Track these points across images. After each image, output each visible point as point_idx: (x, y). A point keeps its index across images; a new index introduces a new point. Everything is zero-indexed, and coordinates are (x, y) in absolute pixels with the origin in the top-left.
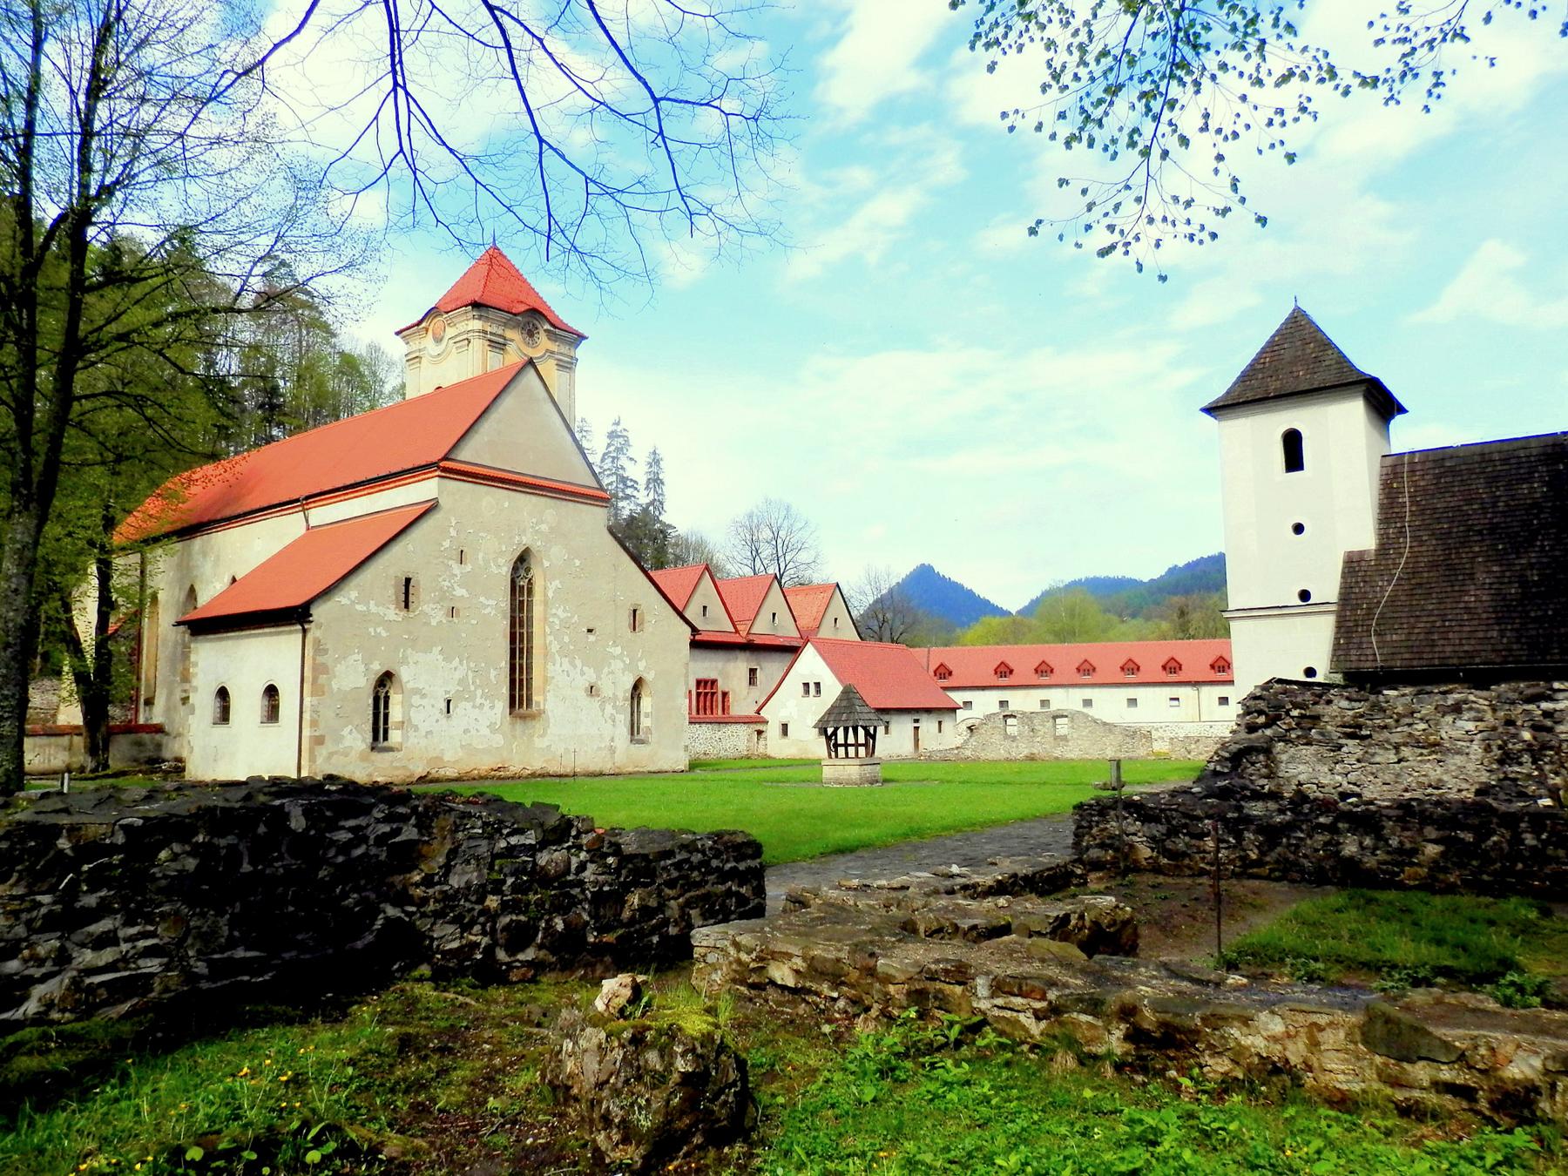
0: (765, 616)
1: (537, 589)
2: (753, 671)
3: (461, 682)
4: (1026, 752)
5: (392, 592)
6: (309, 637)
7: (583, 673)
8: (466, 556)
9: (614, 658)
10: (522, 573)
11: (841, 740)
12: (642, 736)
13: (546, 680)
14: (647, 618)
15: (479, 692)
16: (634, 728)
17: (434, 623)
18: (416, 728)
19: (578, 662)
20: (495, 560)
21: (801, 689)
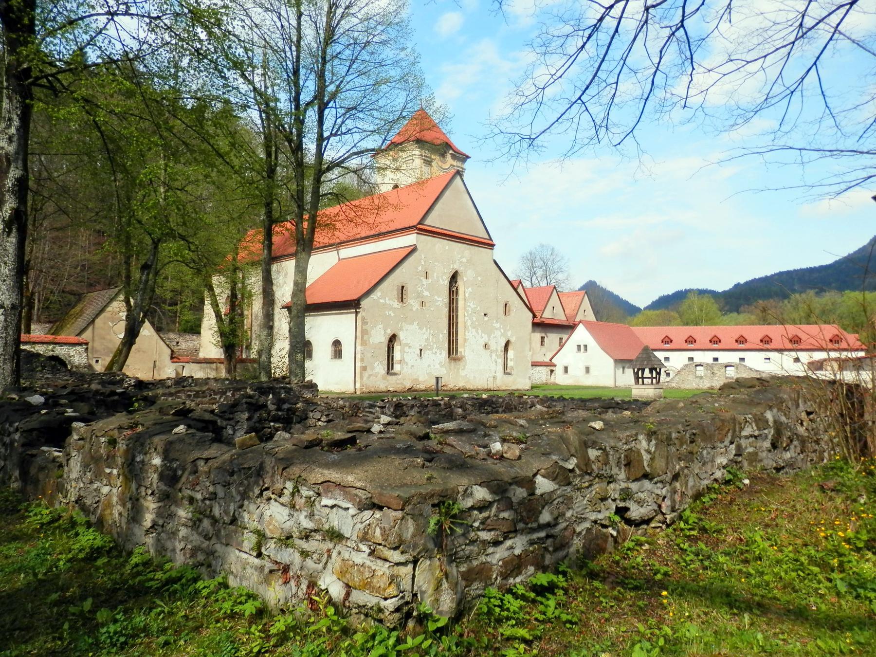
0: (549, 307)
1: (461, 292)
2: (543, 338)
3: (427, 340)
4: (708, 385)
5: (395, 293)
6: (359, 315)
11: (640, 375)
12: (508, 371)
13: (465, 340)
14: (512, 308)
16: (505, 366)
19: (480, 331)
21: (576, 347)
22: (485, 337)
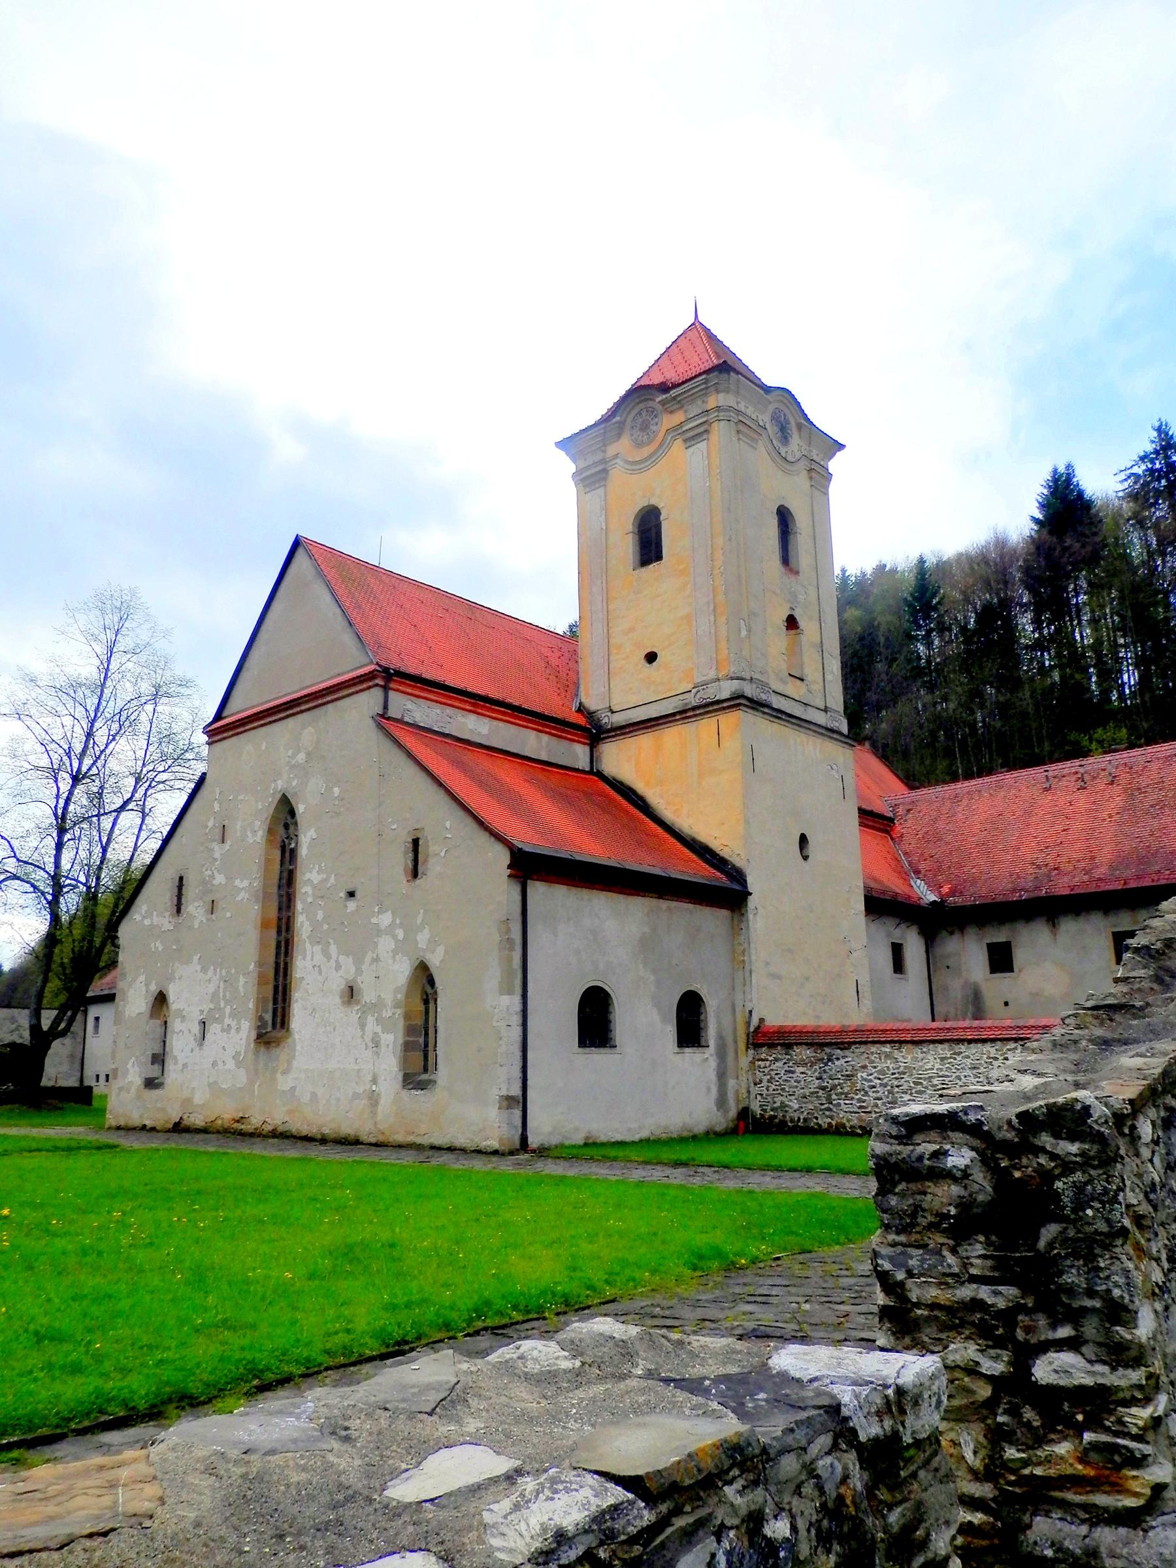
3: (214, 997)
7: (338, 967)
9: (379, 932)
14: (433, 848)
15: (228, 1010)
18: (175, 1058)
19: (333, 949)
22: (347, 962)
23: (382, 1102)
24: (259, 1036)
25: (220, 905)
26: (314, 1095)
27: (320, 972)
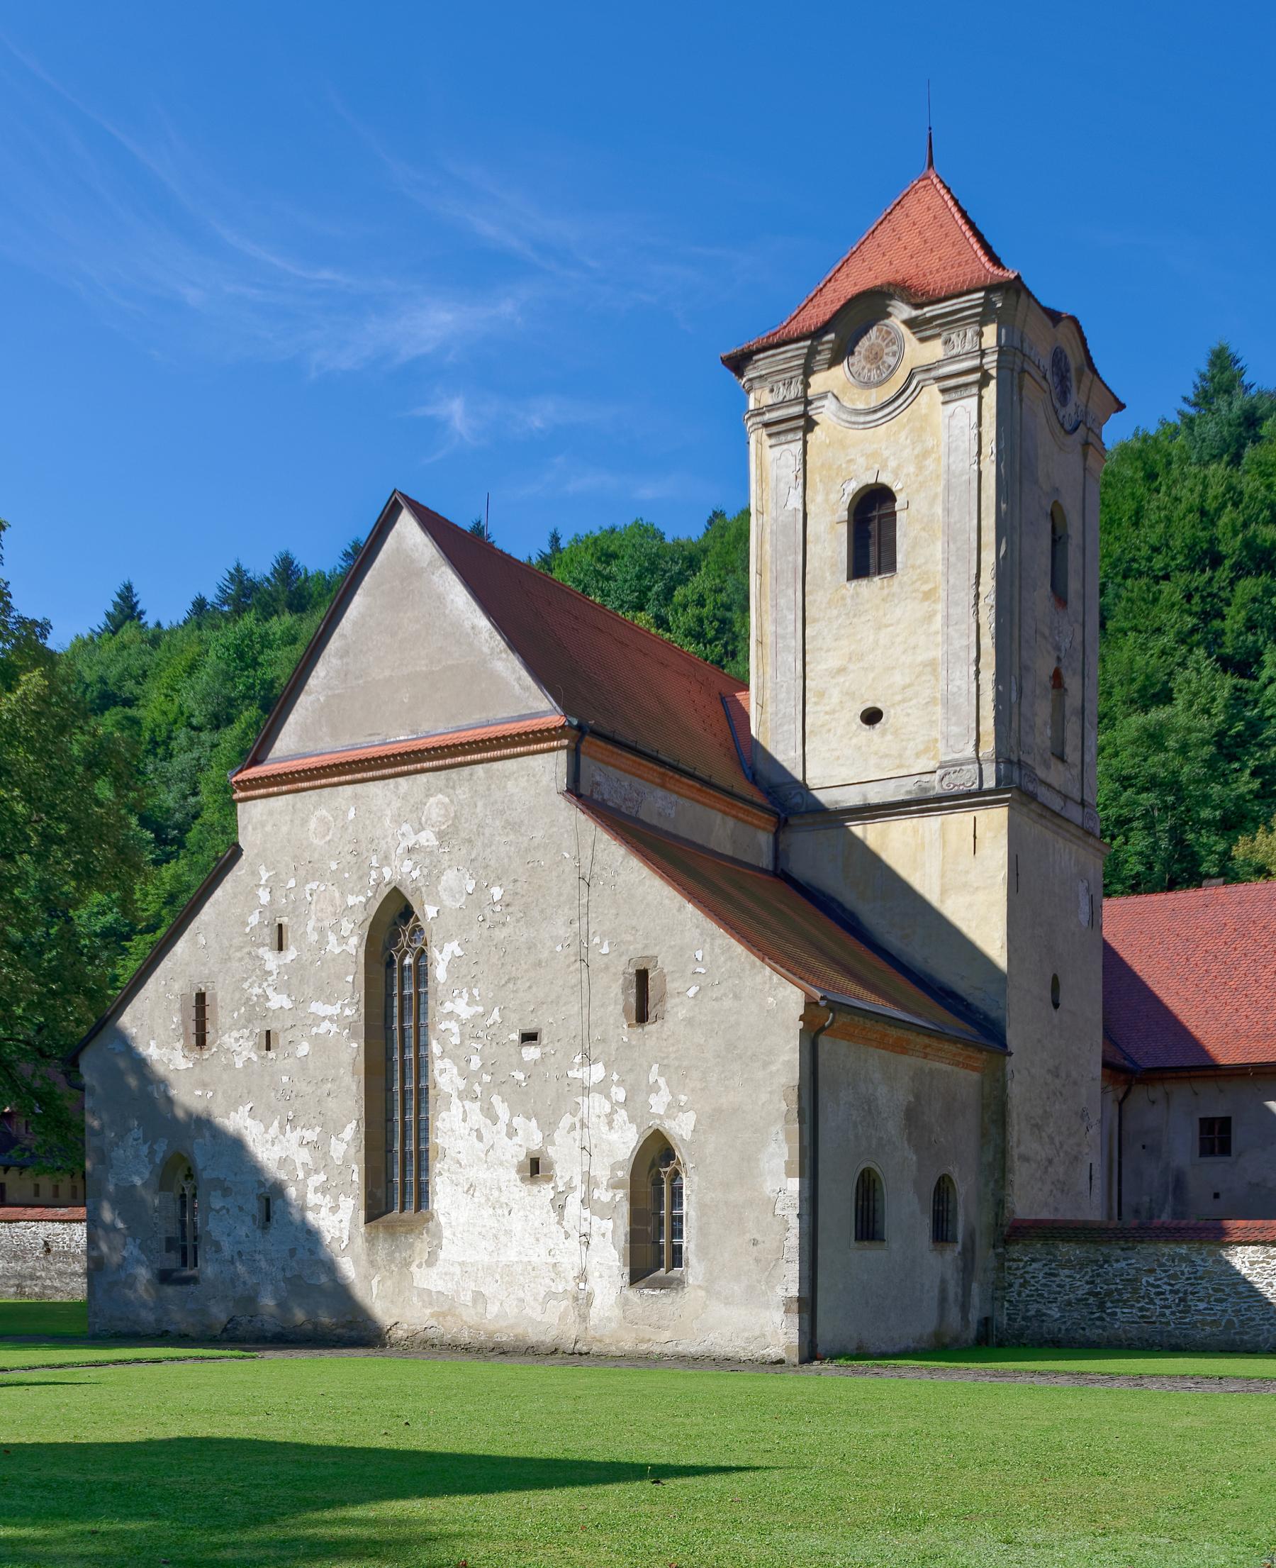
5: (176, 1019)
7: (512, 1132)
8: (289, 937)
9: (586, 1090)
10: (404, 940)
14: (672, 986)
17: (239, 1065)
19: (502, 1110)
20: (336, 928)
23: (597, 1302)
24: (370, 1218)
25: (281, 1040)
26: (479, 1297)
27: (480, 1138)
